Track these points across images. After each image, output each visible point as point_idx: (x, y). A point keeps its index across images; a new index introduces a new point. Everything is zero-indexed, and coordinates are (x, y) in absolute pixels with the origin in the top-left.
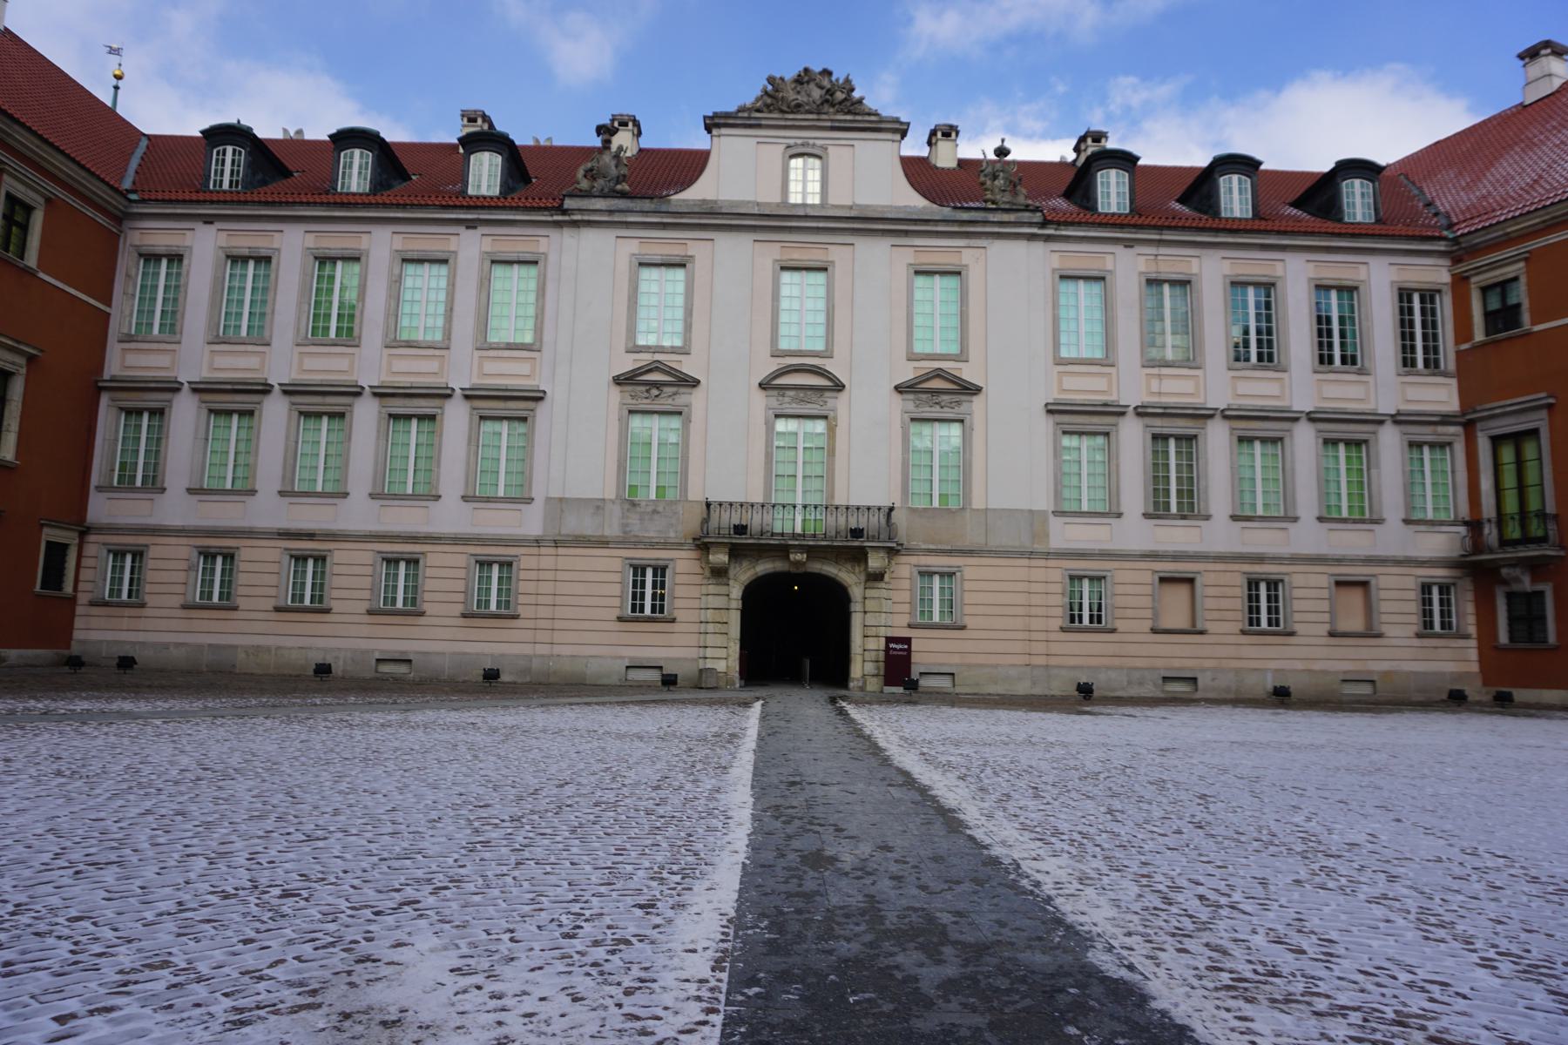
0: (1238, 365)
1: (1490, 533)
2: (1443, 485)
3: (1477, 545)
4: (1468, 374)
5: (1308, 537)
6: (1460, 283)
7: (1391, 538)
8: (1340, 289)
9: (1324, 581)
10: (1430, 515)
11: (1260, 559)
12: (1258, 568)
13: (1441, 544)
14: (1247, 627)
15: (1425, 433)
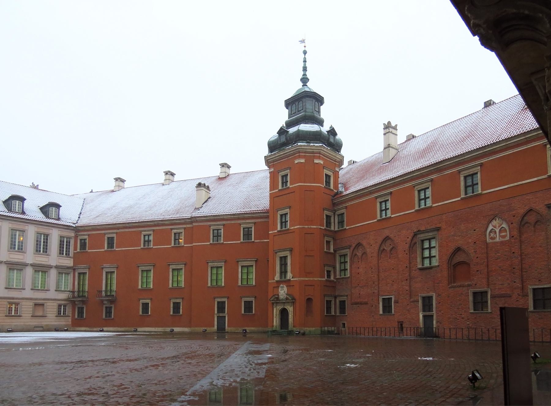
0: (11, 250)
1: (76, 294)
2: (69, 282)
3: (74, 297)
4: (76, 258)
5: (28, 293)
6: (76, 237)
7: (52, 294)
8: (44, 235)
9: (31, 304)
10: (63, 289)
11: (13, 298)
12: (12, 301)
13: (63, 296)
14: (8, 314)
15: (61, 271)
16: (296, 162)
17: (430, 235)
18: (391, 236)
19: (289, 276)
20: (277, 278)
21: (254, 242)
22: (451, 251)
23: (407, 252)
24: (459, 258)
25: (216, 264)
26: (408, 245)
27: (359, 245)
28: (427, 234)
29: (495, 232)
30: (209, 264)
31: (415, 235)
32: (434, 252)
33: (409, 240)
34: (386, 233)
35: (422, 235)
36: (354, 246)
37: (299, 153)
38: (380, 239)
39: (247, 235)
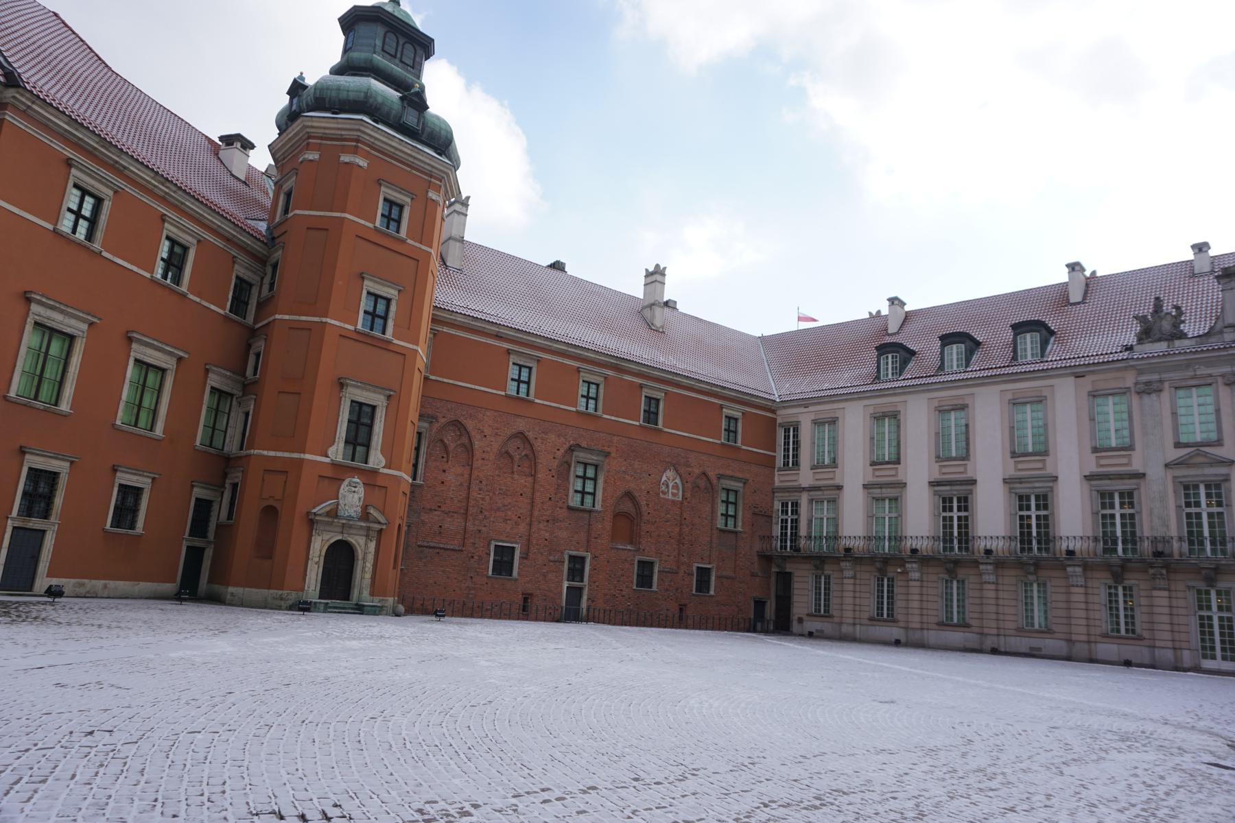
16: (432, 195)
17: (593, 458)
18: (530, 435)
19: (377, 459)
20: (337, 452)
21: (184, 296)
22: (619, 493)
23: (553, 473)
24: (627, 507)
25: (57, 319)
26: (556, 463)
27: (457, 424)
28: (589, 456)
29: (668, 486)
30: (35, 308)
31: (571, 450)
32: (589, 487)
33: (559, 454)
34: (521, 425)
35: (581, 455)
36: (443, 421)
37: (357, 141)
38: (509, 433)
39: (175, 263)
